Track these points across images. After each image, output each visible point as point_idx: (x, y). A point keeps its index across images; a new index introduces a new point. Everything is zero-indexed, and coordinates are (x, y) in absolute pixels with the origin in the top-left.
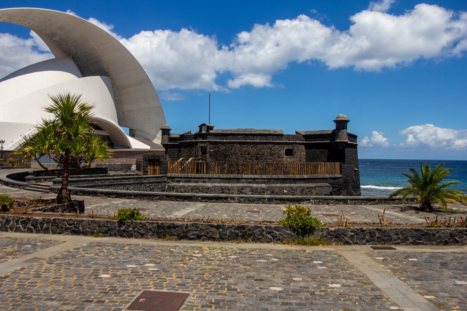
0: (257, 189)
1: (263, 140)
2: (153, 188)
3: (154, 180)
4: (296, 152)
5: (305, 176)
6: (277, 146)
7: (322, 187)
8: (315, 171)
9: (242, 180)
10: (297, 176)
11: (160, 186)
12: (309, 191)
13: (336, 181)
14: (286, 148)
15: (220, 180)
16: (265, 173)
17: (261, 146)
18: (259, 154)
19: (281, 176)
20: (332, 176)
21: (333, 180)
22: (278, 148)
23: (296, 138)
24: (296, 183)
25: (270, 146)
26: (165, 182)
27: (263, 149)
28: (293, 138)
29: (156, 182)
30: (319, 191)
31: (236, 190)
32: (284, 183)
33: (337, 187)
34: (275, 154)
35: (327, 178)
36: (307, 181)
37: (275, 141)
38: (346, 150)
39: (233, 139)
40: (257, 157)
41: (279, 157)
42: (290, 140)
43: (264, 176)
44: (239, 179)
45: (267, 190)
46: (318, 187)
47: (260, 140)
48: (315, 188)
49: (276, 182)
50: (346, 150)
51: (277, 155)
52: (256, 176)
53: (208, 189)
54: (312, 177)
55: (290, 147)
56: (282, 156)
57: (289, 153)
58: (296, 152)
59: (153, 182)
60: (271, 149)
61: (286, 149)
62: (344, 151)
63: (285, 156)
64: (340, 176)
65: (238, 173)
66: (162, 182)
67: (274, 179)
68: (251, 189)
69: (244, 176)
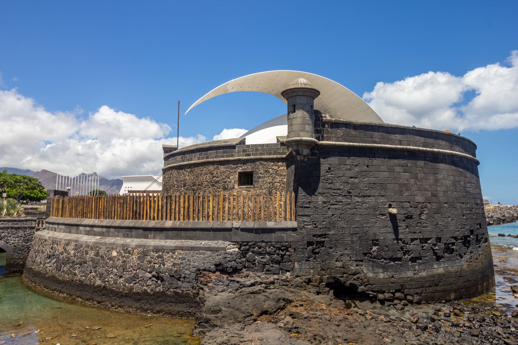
0: (82, 246)
1: (203, 158)
2: (5, 236)
3: (10, 225)
4: (260, 178)
5: (169, 224)
6: (222, 168)
7: (192, 249)
8: (200, 212)
9: (81, 228)
10: (152, 224)
11: (21, 233)
12: (158, 257)
13: (266, 237)
14: (240, 170)
15: (63, 227)
16: (109, 216)
17: (197, 170)
18: (195, 185)
19: (128, 223)
20: (250, 224)
21: (245, 234)
22: (224, 172)
23: (264, 150)
24: (147, 237)
25: (211, 168)
26: (33, 228)
27: (201, 174)
28: (257, 150)
29: (12, 228)
30: (184, 259)
31: (63, 246)
32: (127, 236)
33: (269, 254)
34: (217, 182)
35: (230, 230)
36: (170, 233)
37: (218, 159)
38: (325, 164)
39: (173, 163)
40: (194, 190)
41: (225, 189)
42: (249, 155)
43: (106, 222)
44: (78, 226)
45: (92, 249)
46: (182, 248)
47: (199, 159)
48: (173, 250)
49: (116, 233)
50: (325, 164)
51: (221, 185)
52: (97, 222)
53: (46, 241)
54: (183, 226)
55: (248, 168)
56: (230, 186)
57: (246, 179)
58: (260, 178)
59: (7, 228)
60: (212, 174)
61: (240, 173)
62: (318, 165)
63: (236, 186)
64: (294, 224)
65: (83, 216)
66: (26, 228)
67: (115, 227)
68: (76, 245)
69: (87, 221)
